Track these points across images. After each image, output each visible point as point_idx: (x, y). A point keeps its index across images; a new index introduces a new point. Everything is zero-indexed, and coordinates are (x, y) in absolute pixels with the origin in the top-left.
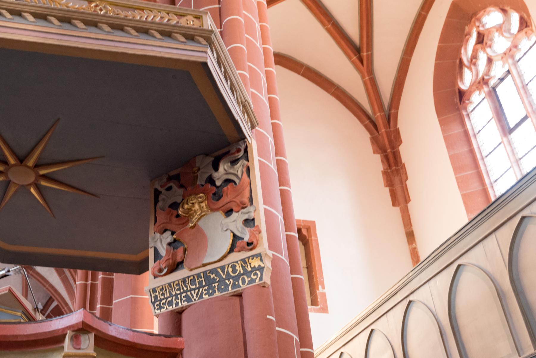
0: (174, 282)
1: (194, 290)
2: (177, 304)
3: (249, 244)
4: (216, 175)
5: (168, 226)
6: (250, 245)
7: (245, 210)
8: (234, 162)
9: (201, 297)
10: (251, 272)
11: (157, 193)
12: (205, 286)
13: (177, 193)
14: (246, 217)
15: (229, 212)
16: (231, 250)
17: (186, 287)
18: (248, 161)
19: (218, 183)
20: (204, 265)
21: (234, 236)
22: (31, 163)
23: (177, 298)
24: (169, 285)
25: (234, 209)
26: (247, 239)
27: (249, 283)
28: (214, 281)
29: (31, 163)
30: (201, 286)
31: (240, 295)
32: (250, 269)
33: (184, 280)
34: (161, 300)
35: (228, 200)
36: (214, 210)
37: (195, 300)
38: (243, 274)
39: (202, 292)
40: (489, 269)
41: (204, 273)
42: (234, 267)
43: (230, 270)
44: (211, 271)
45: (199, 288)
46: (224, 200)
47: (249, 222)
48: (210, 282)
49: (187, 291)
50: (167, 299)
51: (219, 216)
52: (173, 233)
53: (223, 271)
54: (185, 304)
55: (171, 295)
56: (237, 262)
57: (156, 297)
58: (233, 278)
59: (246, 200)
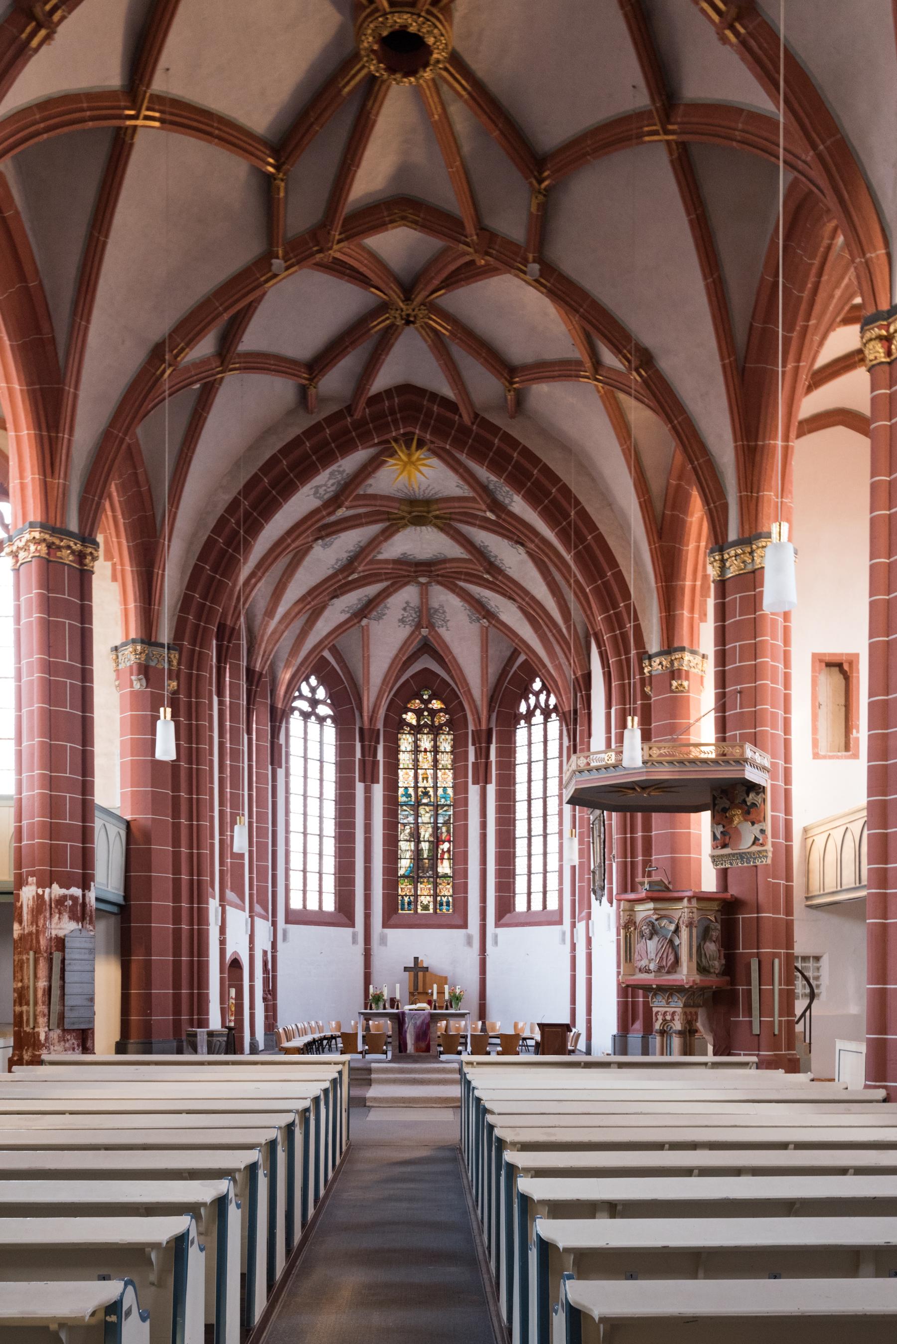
4: (747, 799)
8: (758, 794)
13: (727, 804)
15: (753, 824)
16: (754, 843)
33: (729, 855)
36: (746, 820)
37: (735, 865)
46: (752, 816)
47: (763, 831)
52: (724, 827)
59: (762, 819)
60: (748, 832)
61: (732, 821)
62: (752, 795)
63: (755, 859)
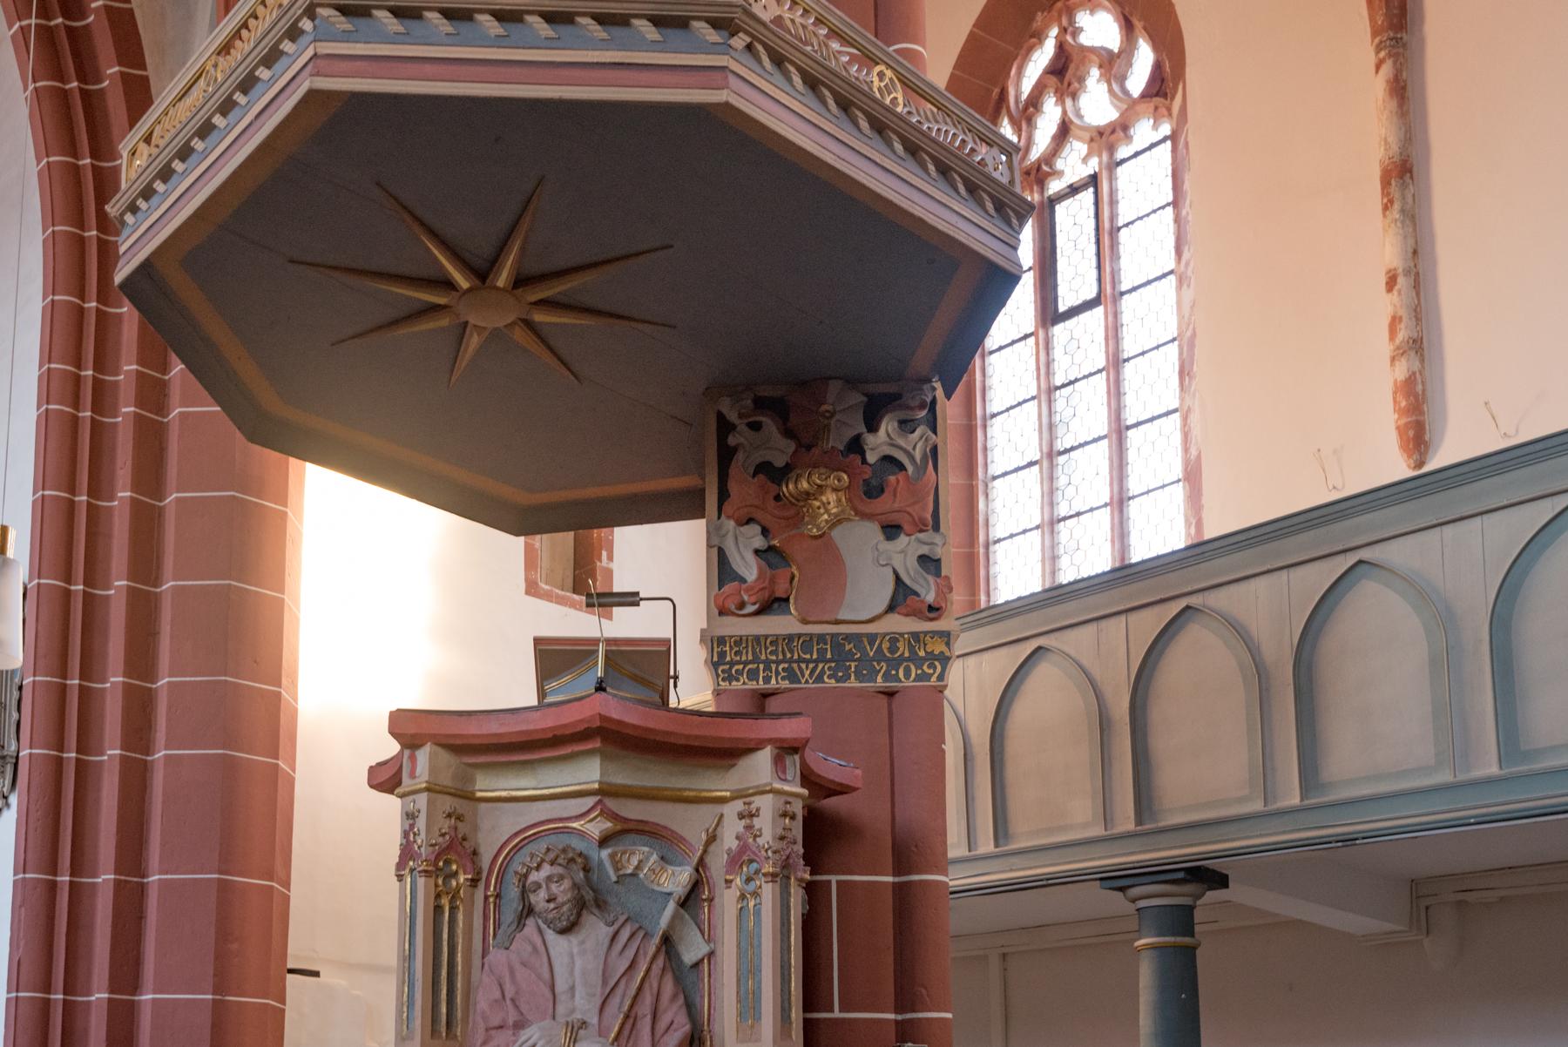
0: (766, 637)
1: (807, 662)
2: (767, 680)
3: (931, 608)
4: (870, 440)
5: (758, 515)
6: (934, 610)
7: (921, 536)
8: (906, 425)
9: (820, 679)
10: (925, 659)
11: (724, 427)
12: (830, 661)
14: (925, 550)
15: (891, 530)
16: (891, 608)
17: (792, 652)
18: (935, 432)
19: (872, 458)
20: (838, 622)
21: (898, 579)
22: (503, 279)
24: (757, 638)
25: (906, 527)
26: (930, 598)
27: (918, 678)
29: (503, 279)
31: (890, 694)
32: (922, 653)
33: (790, 638)
34: (732, 664)
35: (896, 506)
37: (807, 683)
40: (1096, 673)
41: (833, 635)
42: (894, 641)
43: (885, 645)
44: (848, 637)
45: (817, 662)
46: (883, 504)
47: (929, 563)
48: (841, 658)
49: (791, 661)
50: (746, 663)
51: (872, 531)
53: (871, 644)
54: (785, 684)
55: (756, 660)
56: (902, 635)
57: (722, 655)
58: (887, 660)
60: (868, 567)
61: (796, 520)
62: (888, 426)
63: (895, 663)
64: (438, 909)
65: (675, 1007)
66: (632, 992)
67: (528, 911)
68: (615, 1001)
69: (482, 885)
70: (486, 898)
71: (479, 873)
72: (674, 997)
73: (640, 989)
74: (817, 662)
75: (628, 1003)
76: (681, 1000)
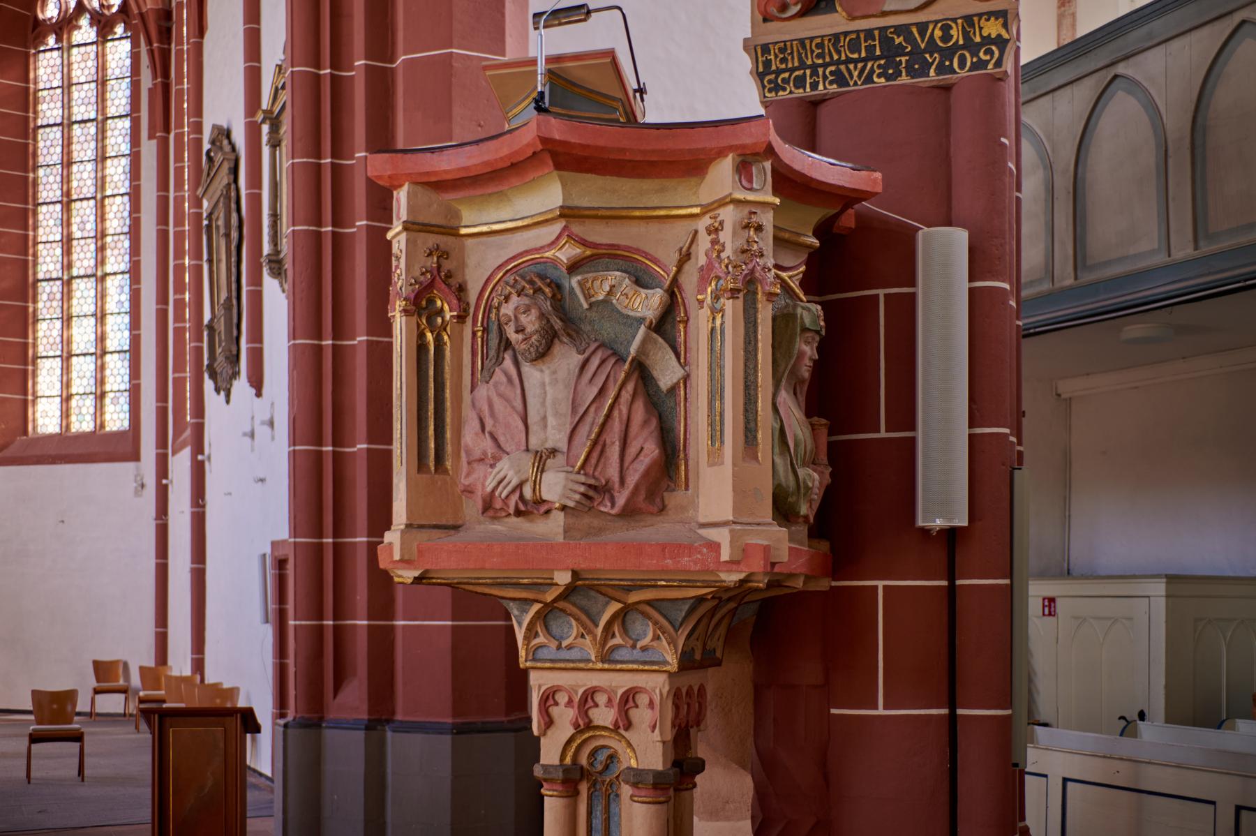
0: (812, 39)
1: (856, 61)
2: (814, 86)
9: (869, 79)
10: (980, 45)
12: (879, 58)
17: (839, 53)
23: (814, 73)
24: (802, 42)
27: (974, 67)
28: (900, 50)
30: (871, 57)
32: (978, 39)
34: (778, 72)
37: (856, 84)
38: (963, 47)
39: (872, 71)
41: (883, 30)
42: (946, 29)
43: (938, 33)
44: (902, 30)
45: (865, 60)
49: (839, 62)
50: (792, 70)
53: (922, 35)
55: (803, 66)
57: (767, 64)
63: (948, 53)
64: (421, 348)
65: (645, 433)
66: (601, 420)
67: (507, 344)
68: (583, 430)
69: (469, 320)
70: (474, 334)
71: (466, 310)
72: (646, 422)
73: (608, 416)
74: (865, 60)
75: (596, 430)
76: (654, 423)
